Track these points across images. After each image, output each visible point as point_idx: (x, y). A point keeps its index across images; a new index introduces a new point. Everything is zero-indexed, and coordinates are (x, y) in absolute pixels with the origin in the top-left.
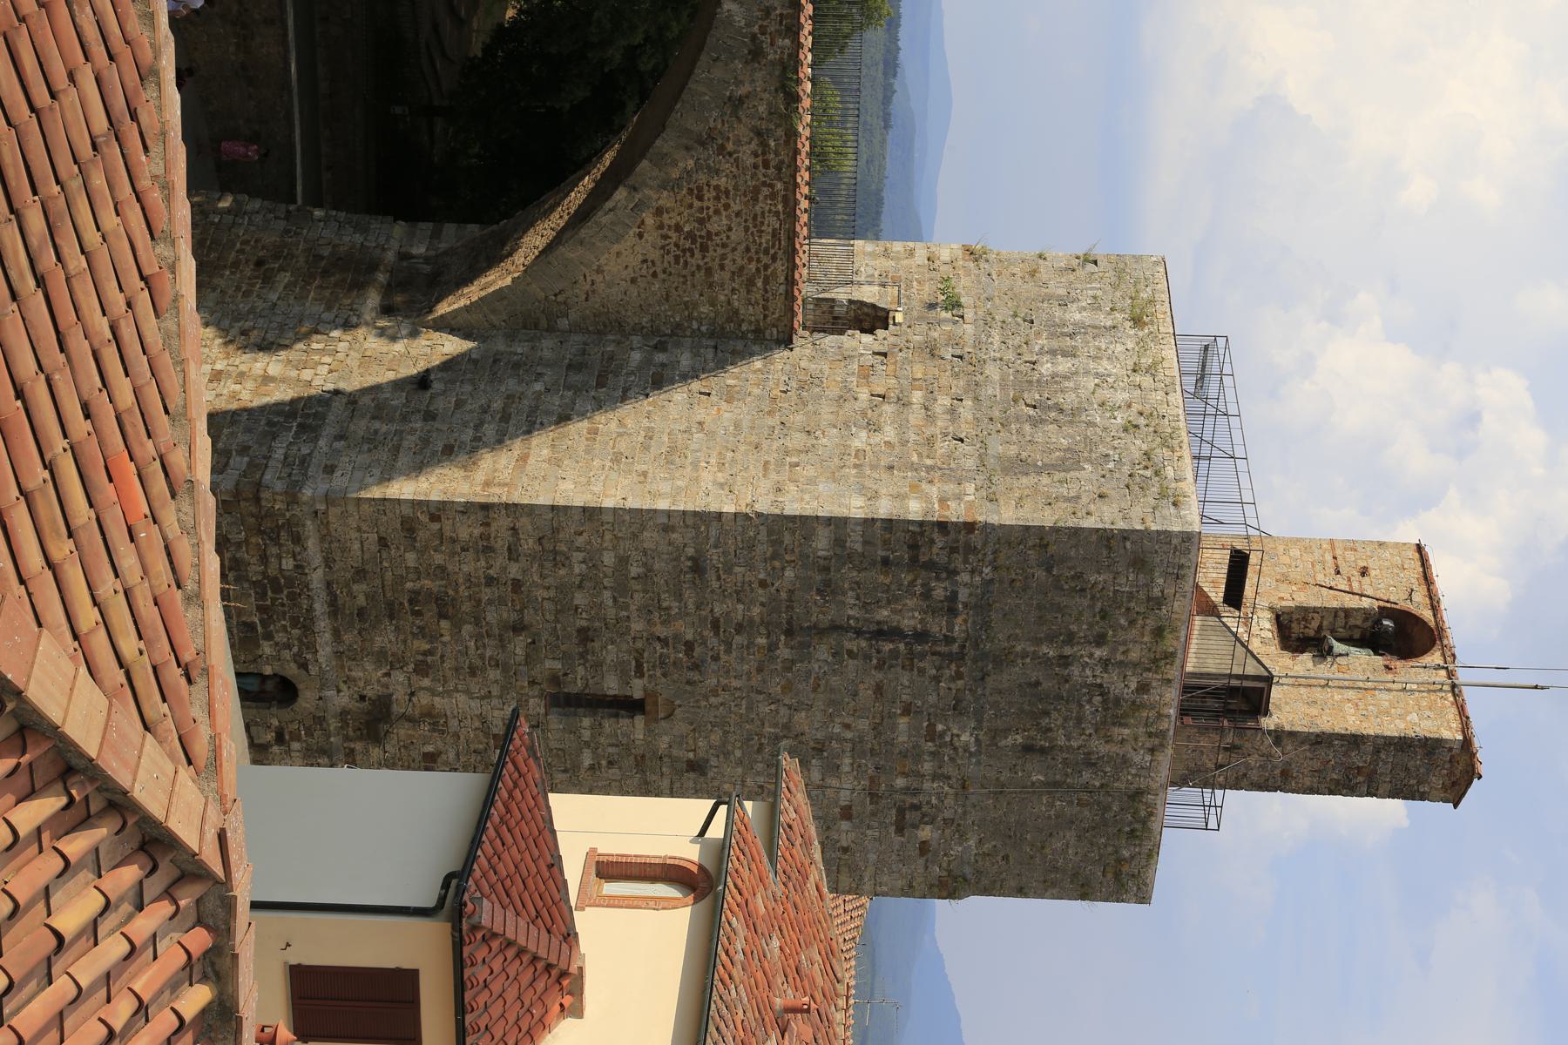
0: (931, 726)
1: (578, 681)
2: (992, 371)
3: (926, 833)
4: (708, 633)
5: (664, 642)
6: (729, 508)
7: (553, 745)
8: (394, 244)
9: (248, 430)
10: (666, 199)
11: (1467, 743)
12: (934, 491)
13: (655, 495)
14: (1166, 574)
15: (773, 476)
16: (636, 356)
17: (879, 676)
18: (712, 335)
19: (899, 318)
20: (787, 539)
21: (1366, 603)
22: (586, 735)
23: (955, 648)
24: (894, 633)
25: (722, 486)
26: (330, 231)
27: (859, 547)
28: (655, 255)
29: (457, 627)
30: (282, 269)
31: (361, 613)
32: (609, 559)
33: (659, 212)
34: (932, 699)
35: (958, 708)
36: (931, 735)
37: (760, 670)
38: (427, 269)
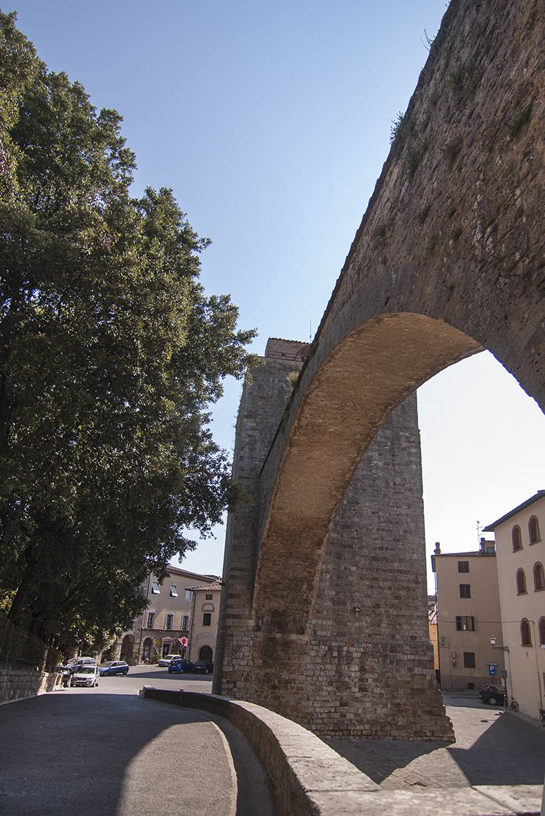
9: (397, 671)
15: (402, 491)
25: (409, 507)
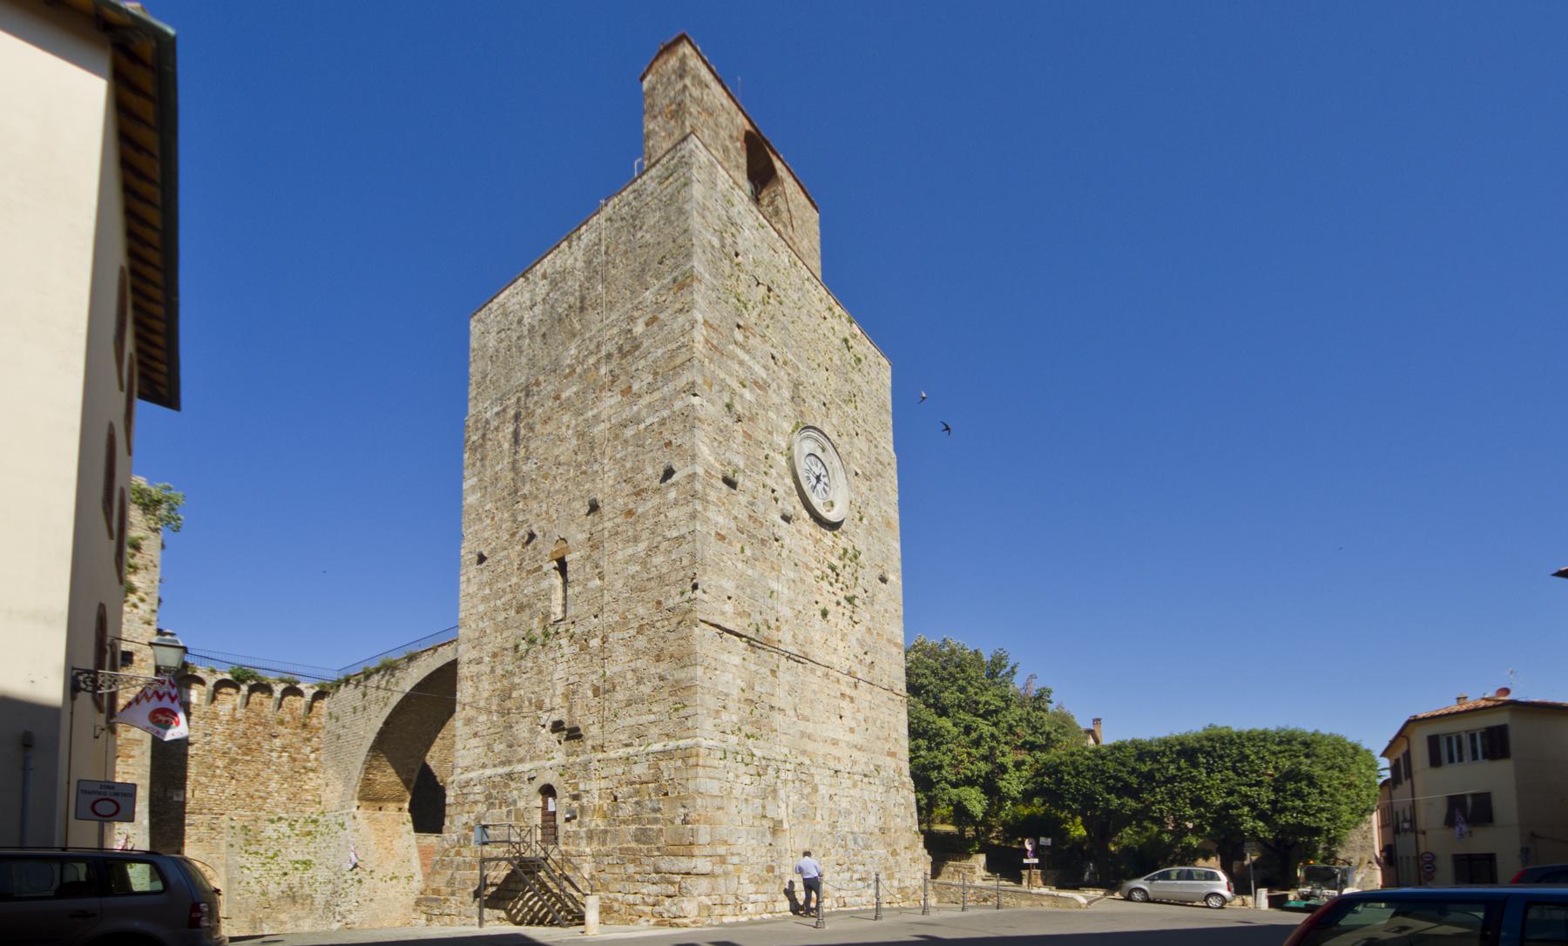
31: (510, 746)
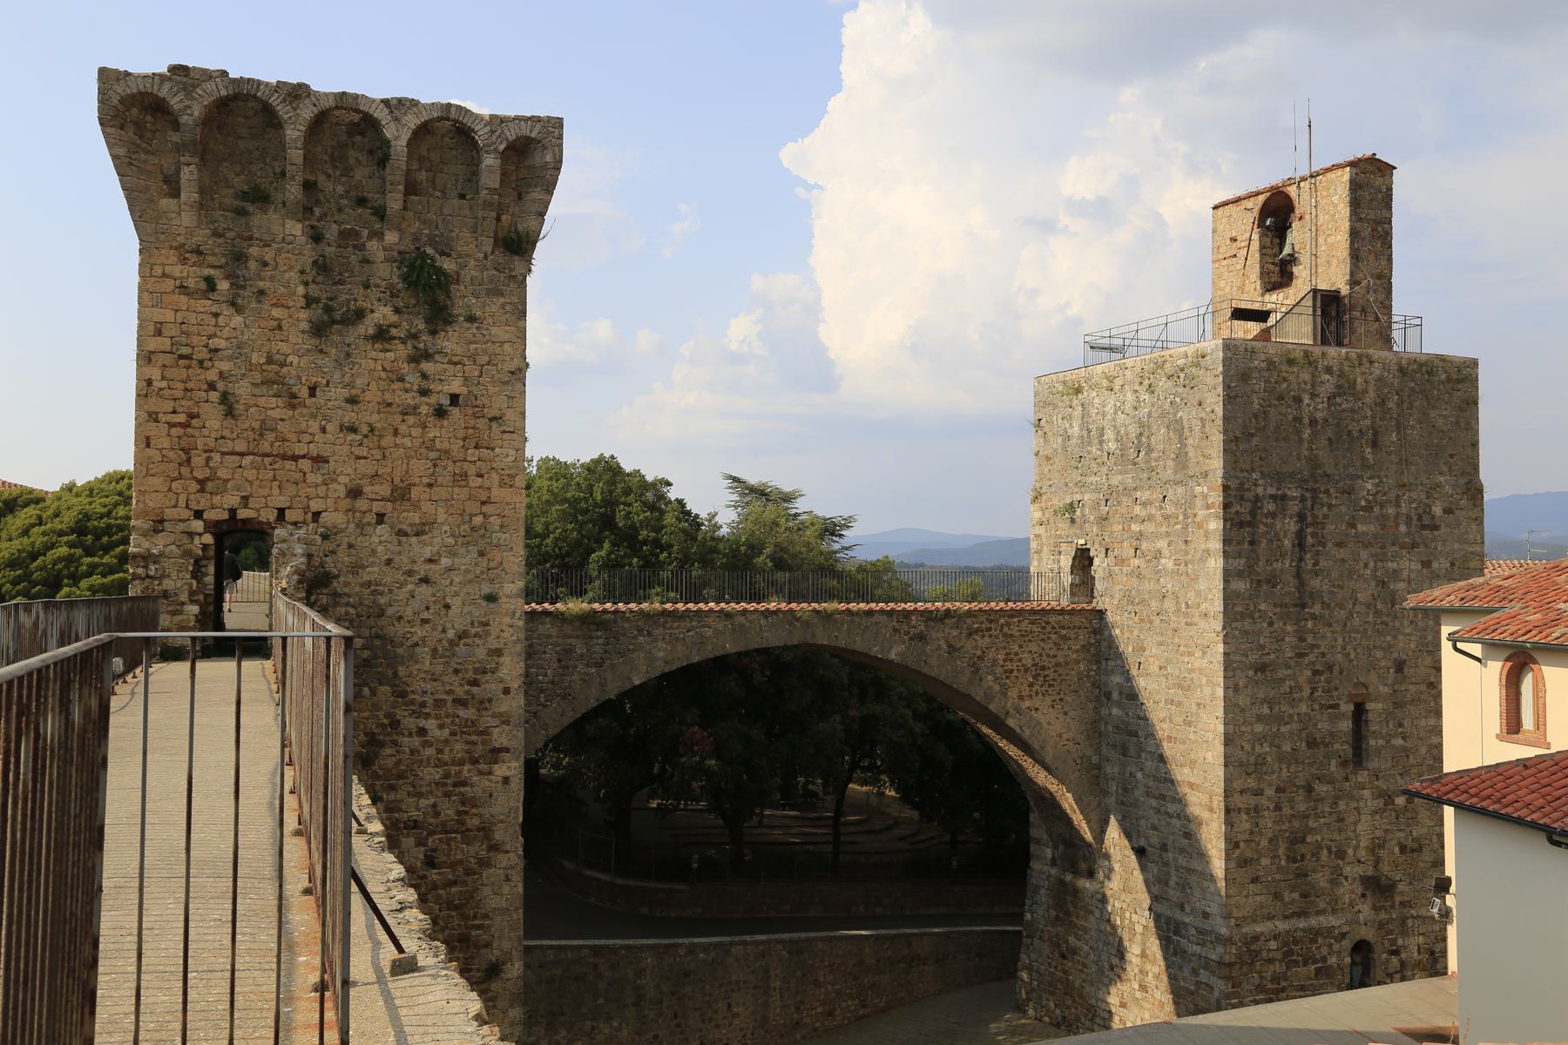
0: (1362, 509)
1: (1343, 748)
2: (1116, 480)
3: (1437, 510)
4: (1306, 660)
5: (1314, 690)
6: (1221, 648)
7: (1389, 765)
8: (1046, 868)
9: (1181, 969)
10: (1013, 693)
11: (1352, 164)
12: (1202, 513)
13: (1213, 696)
14: (1251, 360)
15: (1196, 619)
16: (1115, 711)
17: (1330, 545)
18: (1098, 662)
19: (1082, 541)
20: (1239, 609)
21: (1256, 237)
22: (1381, 742)
23: (1308, 495)
24: (1300, 535)
25: (1204, 653)
26: (1039, 910)
27: (1243, 561)
28: (1048, 700)
29: (1310, 831)
30: (1067, 942)
31: (1304, 896)
32: (1259, 728)
33: (1021, 698)
34: (1344, 509)
35: (1349, 492)
36: (1369, 508)
37: (1330, 625)
38: (1061, 848)
